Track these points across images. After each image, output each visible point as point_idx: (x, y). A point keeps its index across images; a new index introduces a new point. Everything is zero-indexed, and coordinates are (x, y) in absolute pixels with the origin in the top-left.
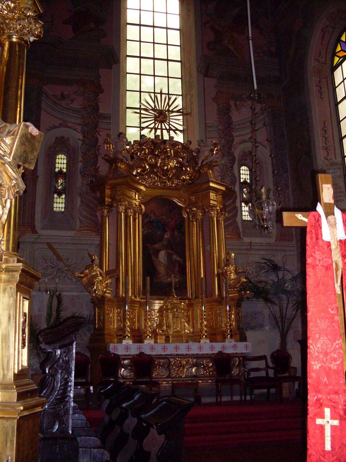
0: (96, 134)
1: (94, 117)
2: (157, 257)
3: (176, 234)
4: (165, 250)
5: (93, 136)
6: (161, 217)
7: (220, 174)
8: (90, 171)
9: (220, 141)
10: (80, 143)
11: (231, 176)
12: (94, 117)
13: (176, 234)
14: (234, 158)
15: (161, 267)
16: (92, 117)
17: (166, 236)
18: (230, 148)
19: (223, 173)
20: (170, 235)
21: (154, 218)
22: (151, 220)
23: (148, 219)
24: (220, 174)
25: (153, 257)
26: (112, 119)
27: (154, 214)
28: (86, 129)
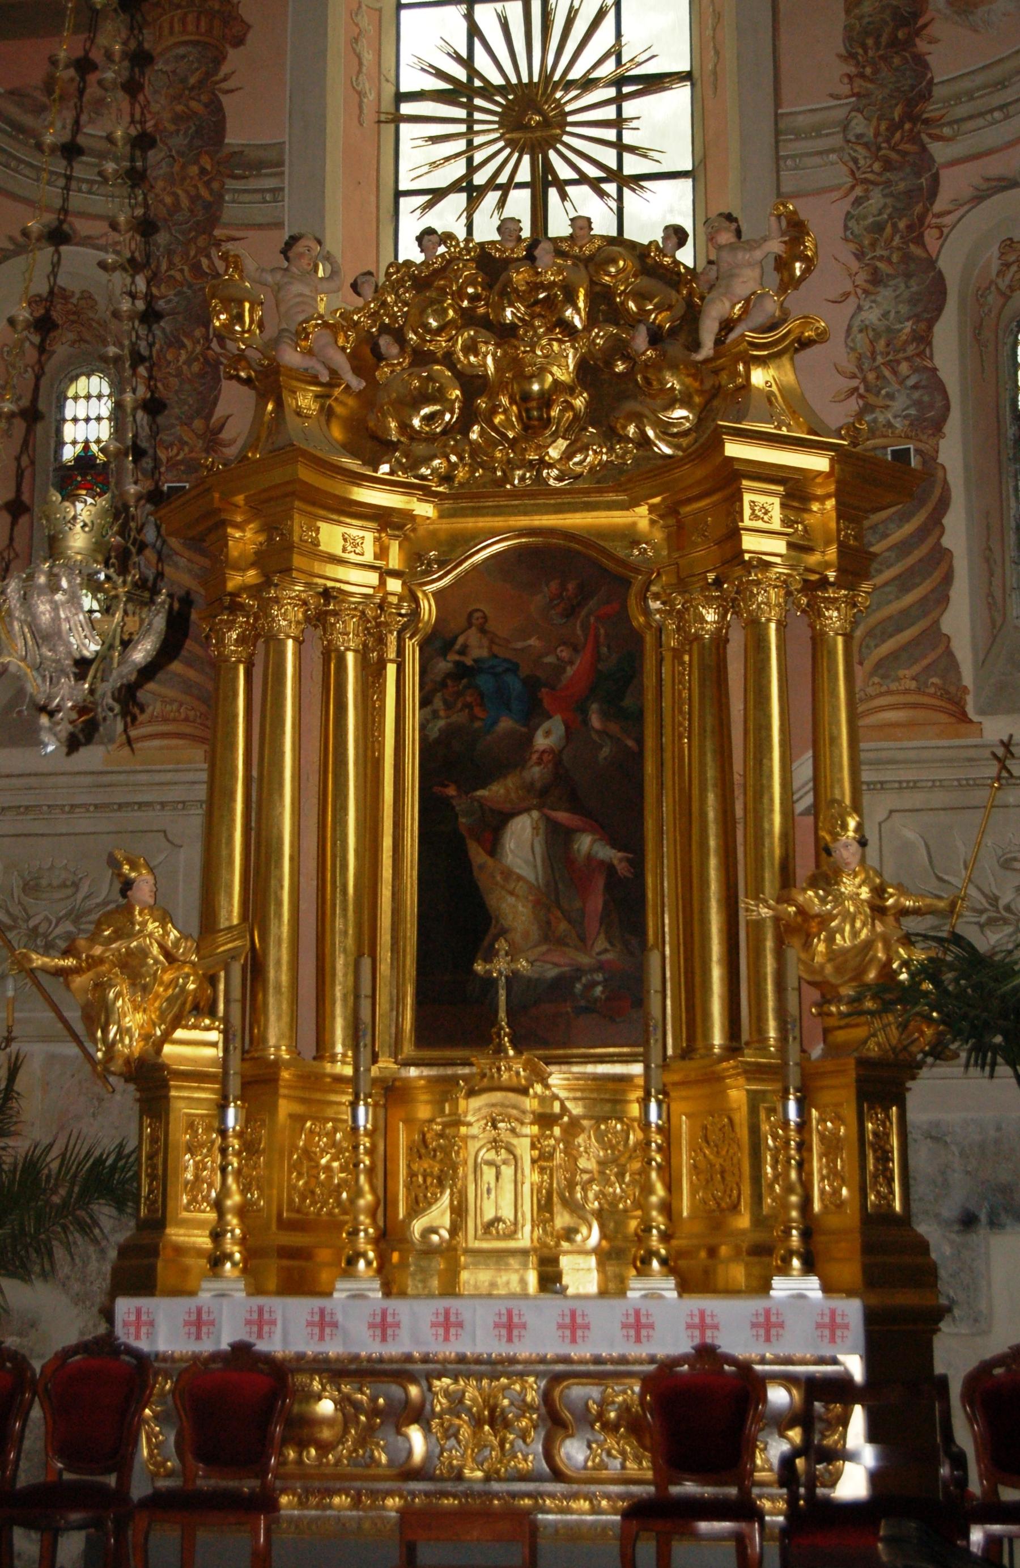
0: (208, 257)
1: (203, 171)
2: (494, 848)
3: (596, 722)
4: (535, 814)
5: (196, 268)
6: (519, 645)
7: (855, 383)
8: (183, 443)
9: (858, 202)
11: (915, 387)
12: (203, 171)
14: (938, 289)
15: (511, 900)
16: (194, 170)
17: (541, 742)
18: (915, 233)
19: (871, 376)
20: (563, 728)
21: (484, 653)
22: (469, 662)
23: (453, 657)
24: (855, 383)
25: (477, 855)
26: (286, 169)
27: (482, 630)
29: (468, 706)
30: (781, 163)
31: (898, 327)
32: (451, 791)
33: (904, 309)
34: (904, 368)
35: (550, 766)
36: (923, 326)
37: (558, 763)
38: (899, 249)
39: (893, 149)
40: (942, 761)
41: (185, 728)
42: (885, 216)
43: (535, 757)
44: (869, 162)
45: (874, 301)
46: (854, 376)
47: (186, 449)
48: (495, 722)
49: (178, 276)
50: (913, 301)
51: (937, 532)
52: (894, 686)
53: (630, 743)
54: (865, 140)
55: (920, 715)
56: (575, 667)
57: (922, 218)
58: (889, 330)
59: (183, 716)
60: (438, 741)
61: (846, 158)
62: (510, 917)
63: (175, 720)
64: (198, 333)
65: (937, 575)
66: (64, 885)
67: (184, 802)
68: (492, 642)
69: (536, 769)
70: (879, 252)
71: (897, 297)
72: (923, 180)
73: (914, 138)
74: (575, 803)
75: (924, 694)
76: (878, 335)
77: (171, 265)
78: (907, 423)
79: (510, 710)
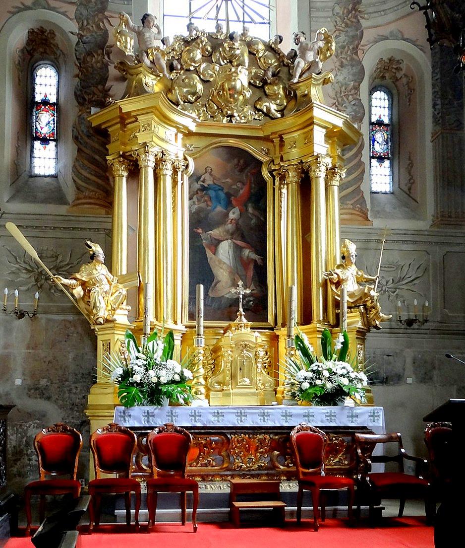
0: (103, 22)
3: (250, 210)
4: (229, 241)
5: (98, 26)
7: (335, 101)
8: (94, 94)
10: (75, 39)
13: (250, 210)
14: (362, 71)
17: (231, 216)
18: (355, 50)
19: (340, 99)
21: (211, 183)
22: (206, 186)
23: (200, 183)
24: (335, 101)
25: (209, 253)
27: (211, 174)
28: (85, 12)
29: (205, 201)
30: (311, 19)
31: (349, 83)
32: (200, 231)
33: (351, 77)
34: (350, 98)
35: (235, 224)
36: (357, 84)
37: (237, 224)
38: (350, 56)
39: (349, 20)
40: (360, 233)
41: (98, 202)
42: (346, 44)
43: (230, 221)
44: (341, 23)
45: (341, 73)
46: (334, 99)
47: (96, 97)
48: (215, 207)
49: (91, 29)
50: (354, 75)
51: (360, 155)
52: (345, 207)
53: (262, 219)
54: (339, 15)
55: (354, 217)
56: (243, 190)
57: (357, 47)
58: (346, 84)
59: (97, 197)
60: (194, 213)
61: (333, 20)
62: (221, 276)
63: (94, 198)
64: (100, 51)
65: (360, 170)
66: (52, 257)
67: (98, 229)
68: (214, 179)
69: (230, 225)
70: (343, 56)
71: (349, 73)
72: (358, 32)
73: (356, 17)
74: (243, 238)
75: (355, 210)
76: (342, 86)
77: (88, 23)
78: (351, 117)
79: (220, 203)
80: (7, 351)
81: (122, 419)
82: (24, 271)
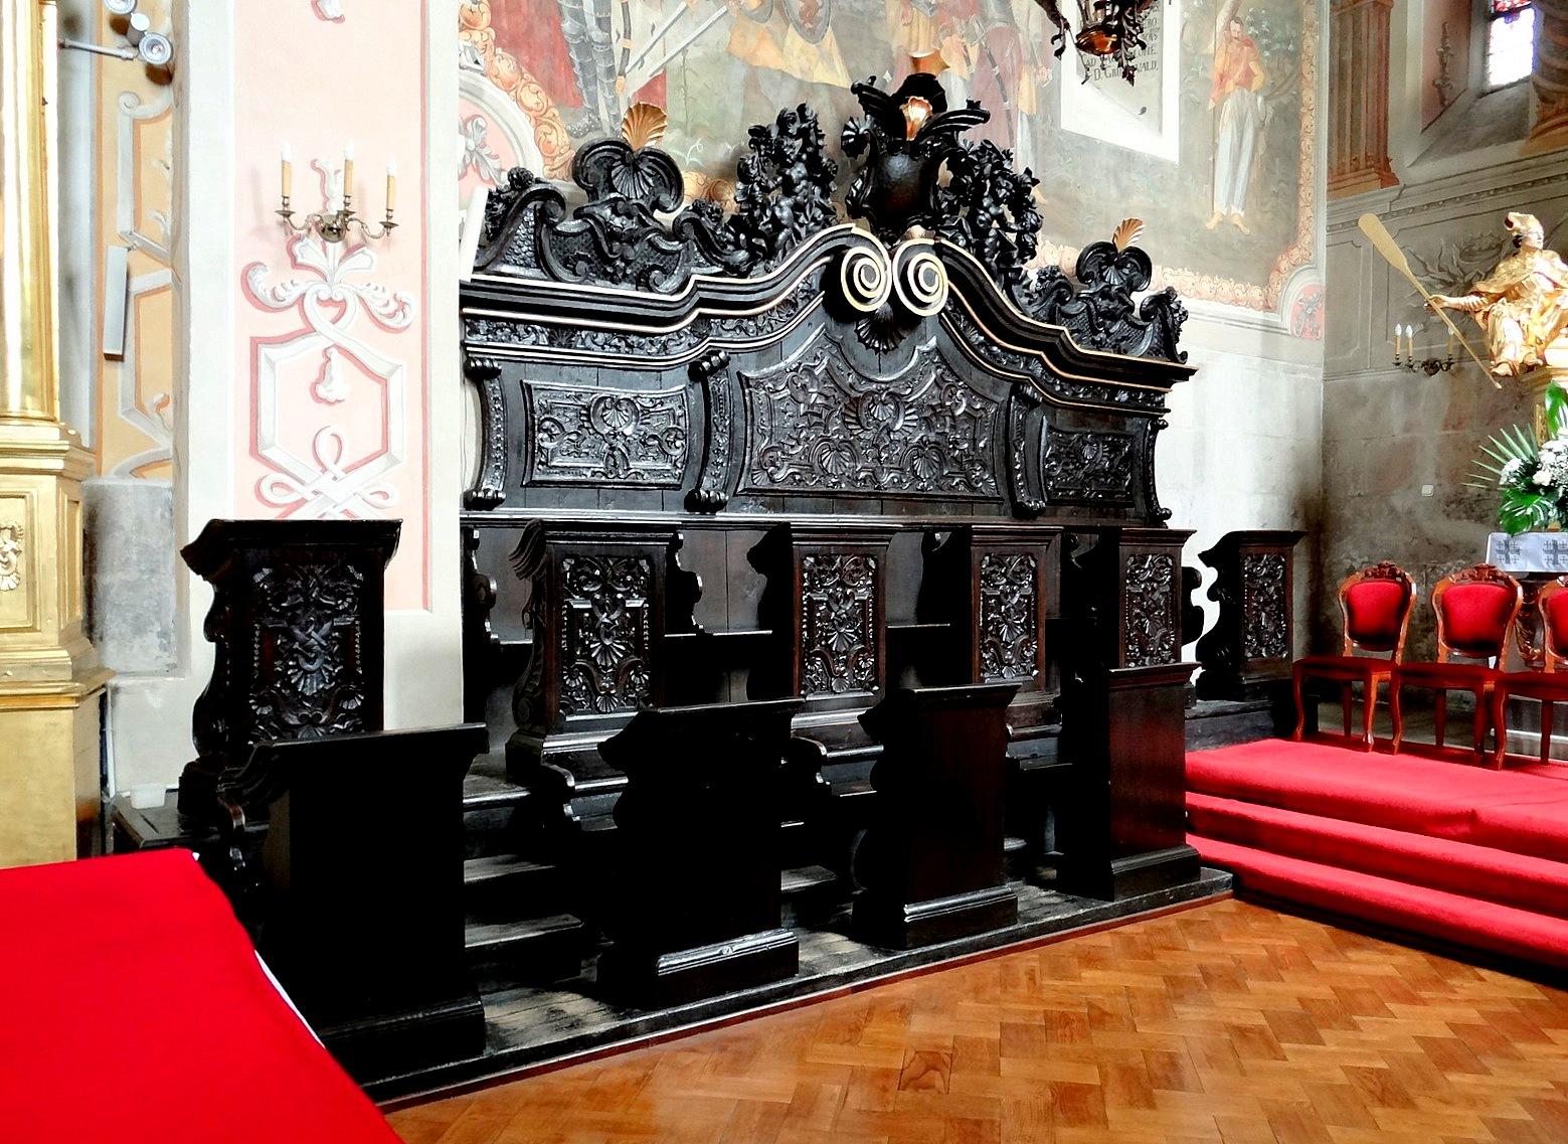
66: (1490, 248)
80: (1408, 435)
81: (1503, 556)
82: (1440, 286)
